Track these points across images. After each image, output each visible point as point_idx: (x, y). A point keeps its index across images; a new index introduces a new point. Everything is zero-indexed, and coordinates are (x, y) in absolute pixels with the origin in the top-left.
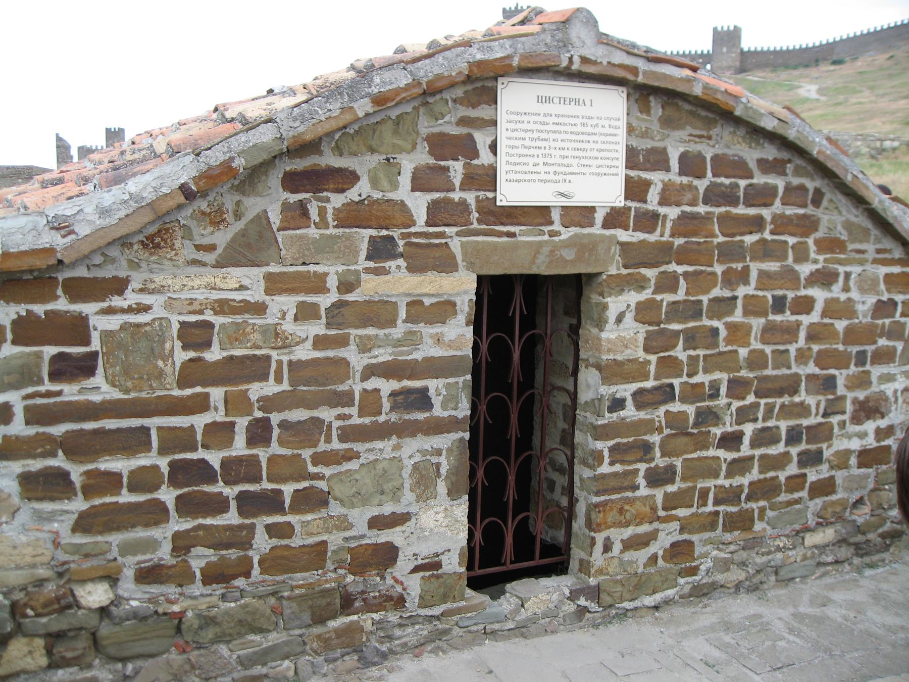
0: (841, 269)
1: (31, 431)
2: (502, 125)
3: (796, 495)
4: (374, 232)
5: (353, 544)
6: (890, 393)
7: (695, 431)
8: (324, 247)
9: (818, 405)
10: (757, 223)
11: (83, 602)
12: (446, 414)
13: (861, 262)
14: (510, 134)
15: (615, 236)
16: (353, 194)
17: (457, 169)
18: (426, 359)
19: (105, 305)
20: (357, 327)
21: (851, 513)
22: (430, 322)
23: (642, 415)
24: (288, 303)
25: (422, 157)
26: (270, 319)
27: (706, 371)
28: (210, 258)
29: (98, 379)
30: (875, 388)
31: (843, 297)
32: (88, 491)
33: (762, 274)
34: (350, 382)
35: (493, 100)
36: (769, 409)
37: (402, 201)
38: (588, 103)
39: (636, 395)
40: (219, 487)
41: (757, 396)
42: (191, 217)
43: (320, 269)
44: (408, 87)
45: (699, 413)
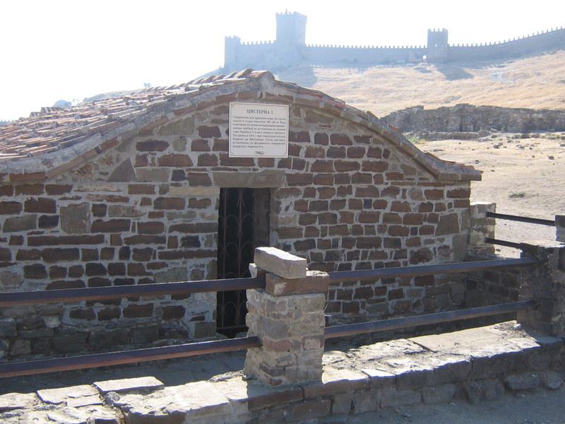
0: (401, 188)
1: (30, 248)
3: (381, 297)
5: (164, 306)
6: (431, 249)
7: (327, 262)
9: (391, 253)
10: (356, 166)
11: (47, 324)
12: (206, 249)
13: (412, 184)
14: (235, 126)
15: (284, 171)
16: (166, 152)
17: (211, 142)
18: (197, 224)
19: (63, 196)
20: (167, 209)
21: (413, 309)
22: (199, 208)
24: (136, 198)
25: (197, 136)
26: (131, 204)
27: (330, 234)
28: (106, 178)
29: (59, 227)
30: (423, 246)
31: (402, 201)
32: (53, 275)
34: (164, 233)
36: (365, 255)
37: (187, 155)
38: (270, 112)
39: (296, 244)
40: (107, 277)
41: (358, 247)
42: (99, 161)
43: (152, 183)
45: (328, 254)
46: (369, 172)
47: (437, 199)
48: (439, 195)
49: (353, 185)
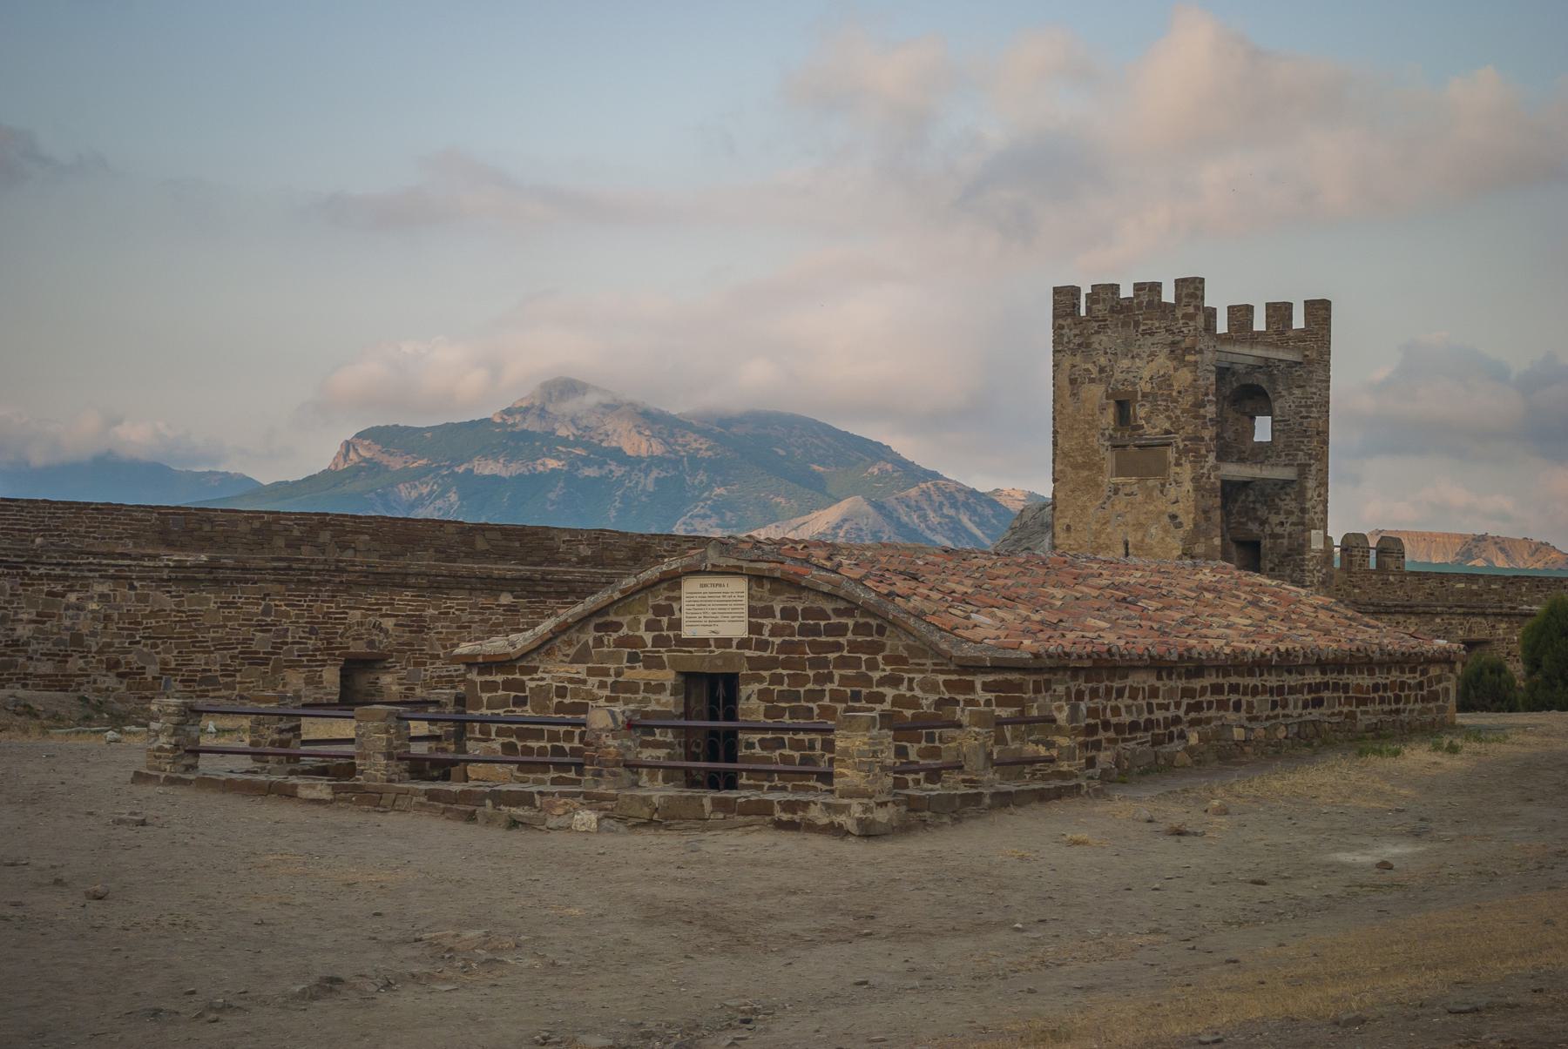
0: (906, 676)
2: (684, 599)
4: (629, 650)
8: (611, 657)
10: (838, 646)
12: (661, 739)
16: (621, 633)
17: (665, 620)
22: (654, 693)
23: (765, 753)
24: (593, 681)
25: (650, 616)
28: (568, 659)
29: (528, 708)
31: (908, 694)
33: (842, 676)
35: (680, 588)
39: (760, 741)
44: (635, 585)
46: (858, 655)
47: (964, 694)
48: (970, 687)
49: (835, 671)
